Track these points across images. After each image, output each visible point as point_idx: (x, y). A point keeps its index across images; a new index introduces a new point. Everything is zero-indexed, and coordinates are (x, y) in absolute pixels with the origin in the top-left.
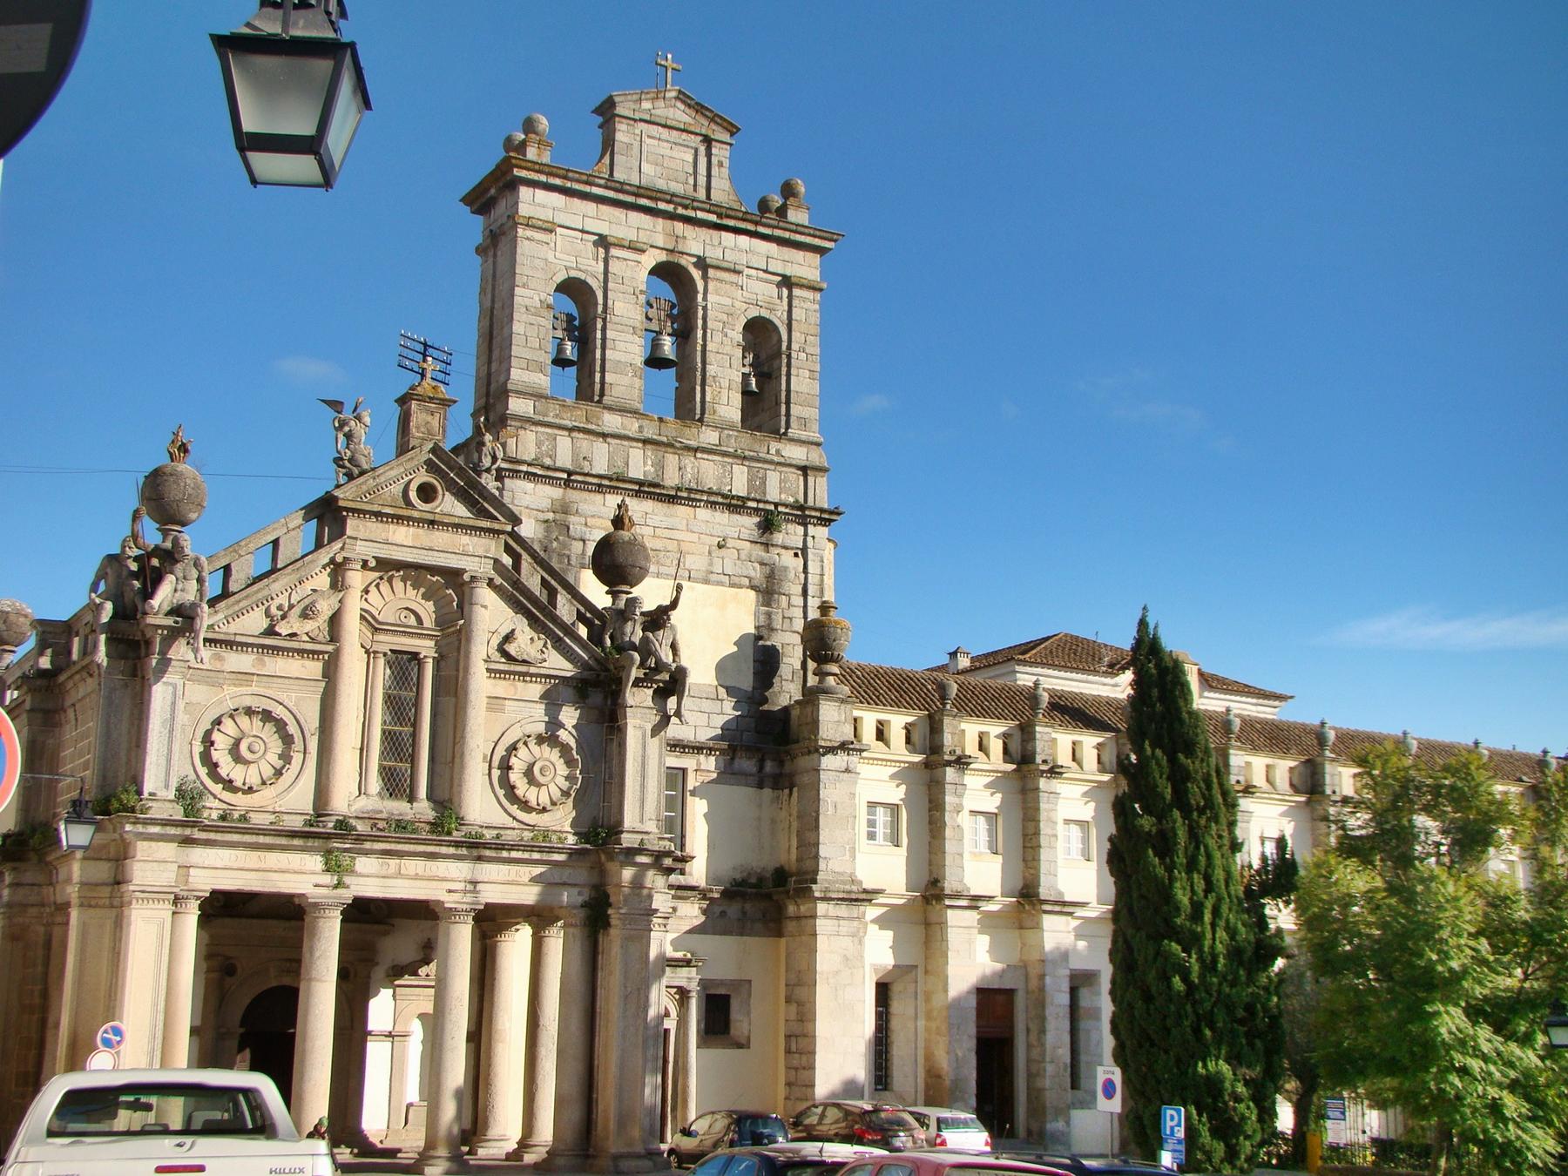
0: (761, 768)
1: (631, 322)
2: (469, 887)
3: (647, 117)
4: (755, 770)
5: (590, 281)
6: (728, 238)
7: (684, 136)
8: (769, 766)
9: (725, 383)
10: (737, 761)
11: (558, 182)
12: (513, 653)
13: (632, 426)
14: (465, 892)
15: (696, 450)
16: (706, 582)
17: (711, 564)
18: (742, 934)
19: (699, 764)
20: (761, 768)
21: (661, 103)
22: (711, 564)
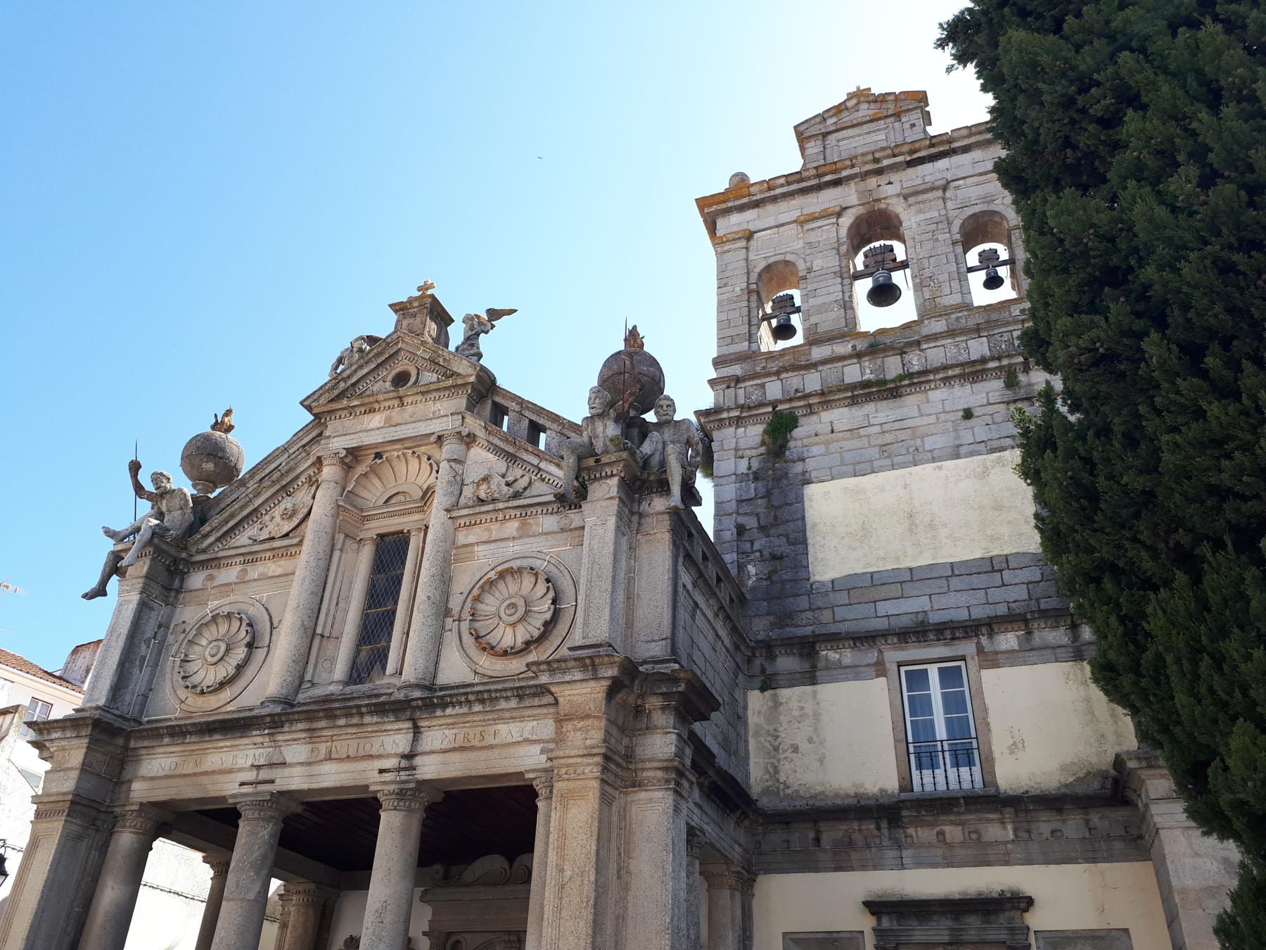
0: (1076, 638)
1: (833, 270)
2: (404, 763)
3: (832, 128)
4: (1066, 640)
5: (789, 257)
6: (927, 168)
7: (874, 124)
8: (1087, 633)
9: (946, 276)
10: (1036, 634)
11: (745, 200)
12: (483, 495)
13: (844, 348)
14: (399, 770)
15: (918, 343)
16: (957, 456)
17: (958, 438)
18: (1094, 860)
19: (980, 650)
20: (1076, 638)
21: (845, 114)
22: (958, 438)
